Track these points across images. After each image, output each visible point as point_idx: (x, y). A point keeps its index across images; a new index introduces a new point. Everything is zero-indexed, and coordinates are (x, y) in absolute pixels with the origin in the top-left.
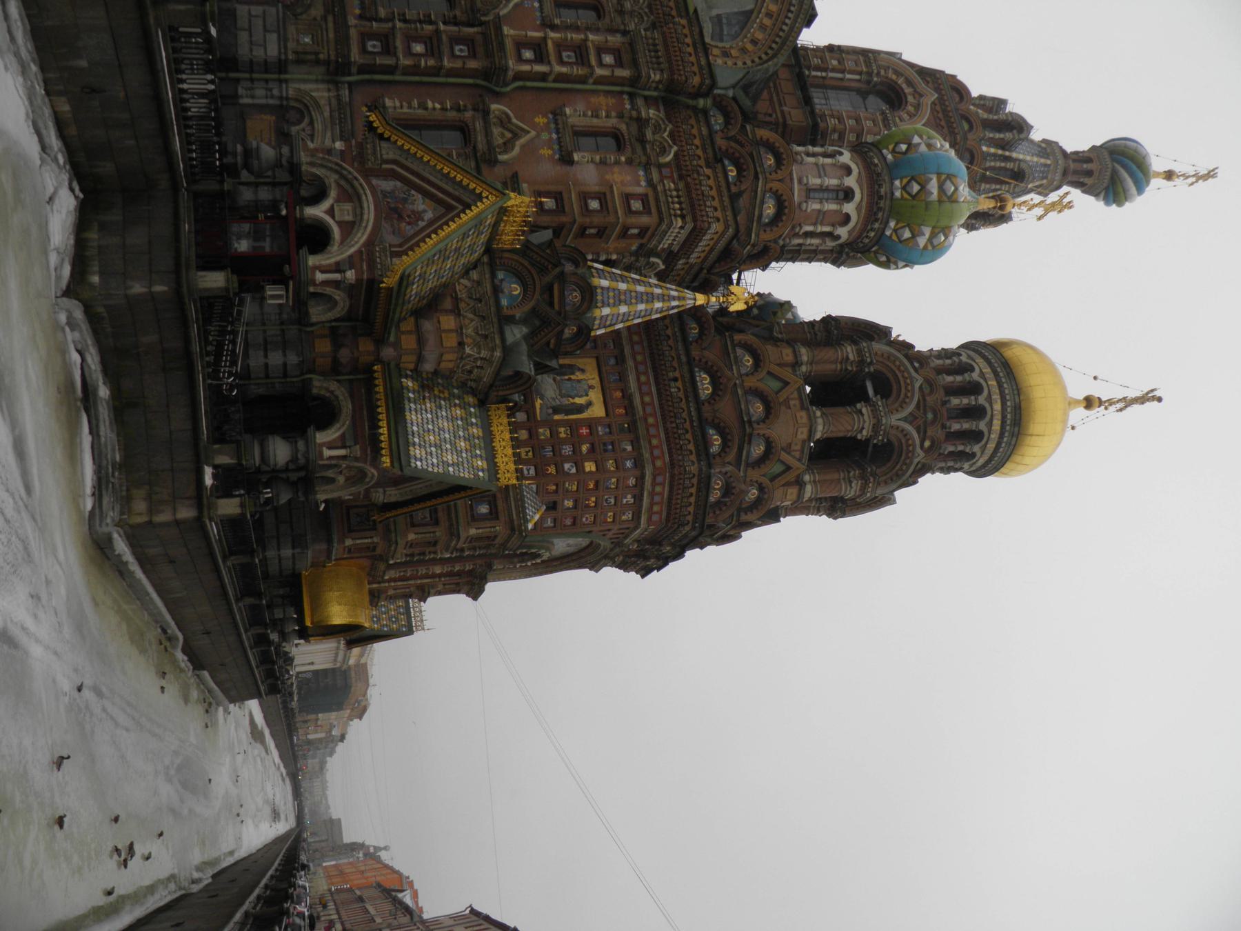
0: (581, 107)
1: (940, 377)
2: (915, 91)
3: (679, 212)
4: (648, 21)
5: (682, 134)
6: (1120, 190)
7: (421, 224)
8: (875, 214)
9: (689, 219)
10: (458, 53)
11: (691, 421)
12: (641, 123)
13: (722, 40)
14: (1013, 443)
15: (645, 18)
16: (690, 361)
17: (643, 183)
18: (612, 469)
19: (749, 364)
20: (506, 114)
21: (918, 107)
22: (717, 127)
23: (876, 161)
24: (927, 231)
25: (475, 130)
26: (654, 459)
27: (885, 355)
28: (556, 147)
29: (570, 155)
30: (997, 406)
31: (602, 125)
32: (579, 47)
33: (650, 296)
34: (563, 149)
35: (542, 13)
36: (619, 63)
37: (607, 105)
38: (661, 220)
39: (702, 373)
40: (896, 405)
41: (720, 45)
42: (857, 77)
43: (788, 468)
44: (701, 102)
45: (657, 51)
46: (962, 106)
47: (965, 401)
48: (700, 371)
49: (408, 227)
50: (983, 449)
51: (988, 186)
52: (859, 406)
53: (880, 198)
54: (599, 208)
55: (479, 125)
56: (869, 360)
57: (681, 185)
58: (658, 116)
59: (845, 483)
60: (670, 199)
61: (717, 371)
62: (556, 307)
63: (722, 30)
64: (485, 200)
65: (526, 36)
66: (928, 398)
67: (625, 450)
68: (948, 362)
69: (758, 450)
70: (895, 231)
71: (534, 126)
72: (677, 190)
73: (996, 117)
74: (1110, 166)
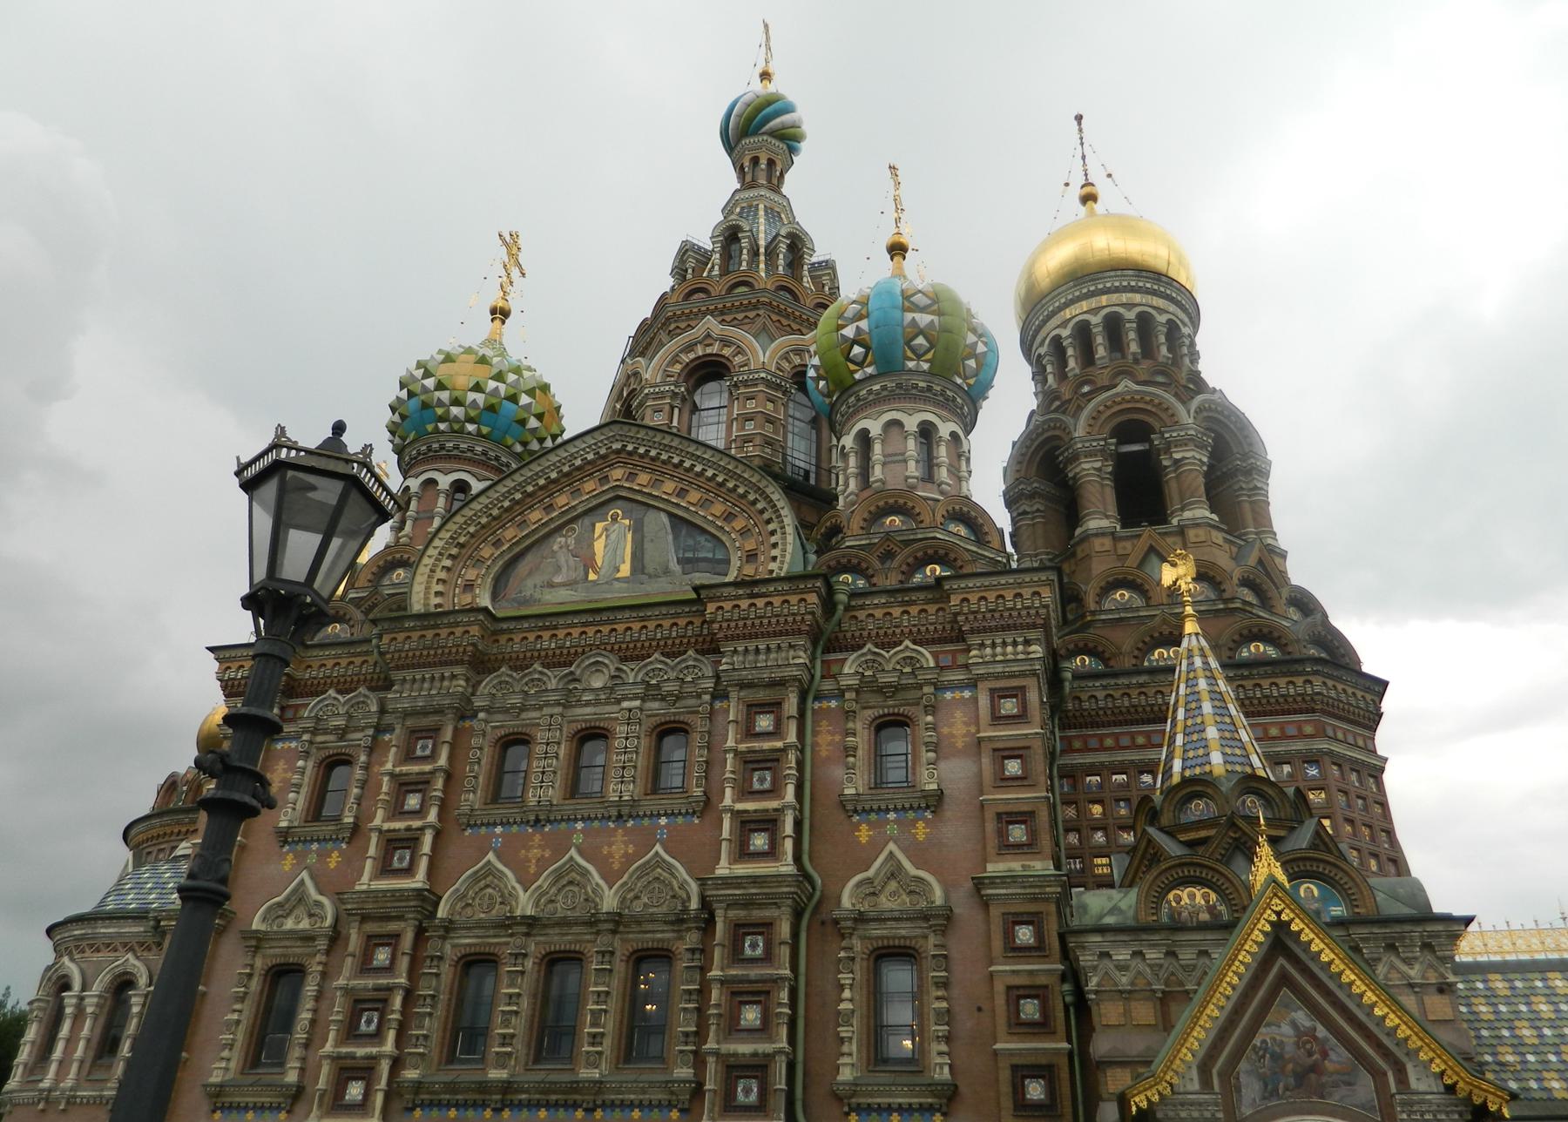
0: (838, 772)
1: (1098, 362)
2: (700, 343)
3: (1020, 648)
4: (695, 660)
5: (882, 632)
6: (792, 130)
7: (1321, 1032)
8: (947, 400)
9: (1032, 635)
10: (759, 951)
11: (1243, 678)
12: (866, 687)
13: (728, 562)
14: (1178, 286)
15: (691, 663)
16: (1139, 671)
17: (967, 694)
18: (1323, 795)
19: (1127, 596)
20: (859, 885)
21: (726, 342)
22: (861, 583)
23: (876, 387)
24: (971, 338)
25: (882, 938)
26: (1302, 736)
27: (1092, 422)
28: (911, 814)
29: (926, 795)
30: (1137, 298)
31: (866, 747)
32: (746, 762)
33: (1214, 696)
34: (915, 805)
35: (680, 814)
36: (774, 707)
37: (833, 735)
38: (1034, 673)
39: (1152, 658)
40: (1163, 416)
41: (735, 562)
42: (676, 411)
43: (1260, 562)
44: (842, 598)
45: (757, 651)
46: (717, 289)
47: (1132, 335)
48: (1149, 660)
49: (1333, 1056)
50: (1185, 325)
51: (805, 279)
52: (1165, 463)
53: (929, 389)
54: (1019, 761)
55: (876, 931)
56: (1102, 443)
57: (975, 640)
58: (853, 661)
59: (1255, 495)
60: (999, 658)
61: (1152, 637)
62: (1282, 833)
63: (705, 560)
64: (1284, 917)
65: (730, 840)
66: (1143, 377)
67: (1290, 775)
68: (1070, 352)
69: (1247, 595)
70: (965, 378)
71: (876, 847)
72: (982, 646)
73: (718, 256)
74: (765, 138)
